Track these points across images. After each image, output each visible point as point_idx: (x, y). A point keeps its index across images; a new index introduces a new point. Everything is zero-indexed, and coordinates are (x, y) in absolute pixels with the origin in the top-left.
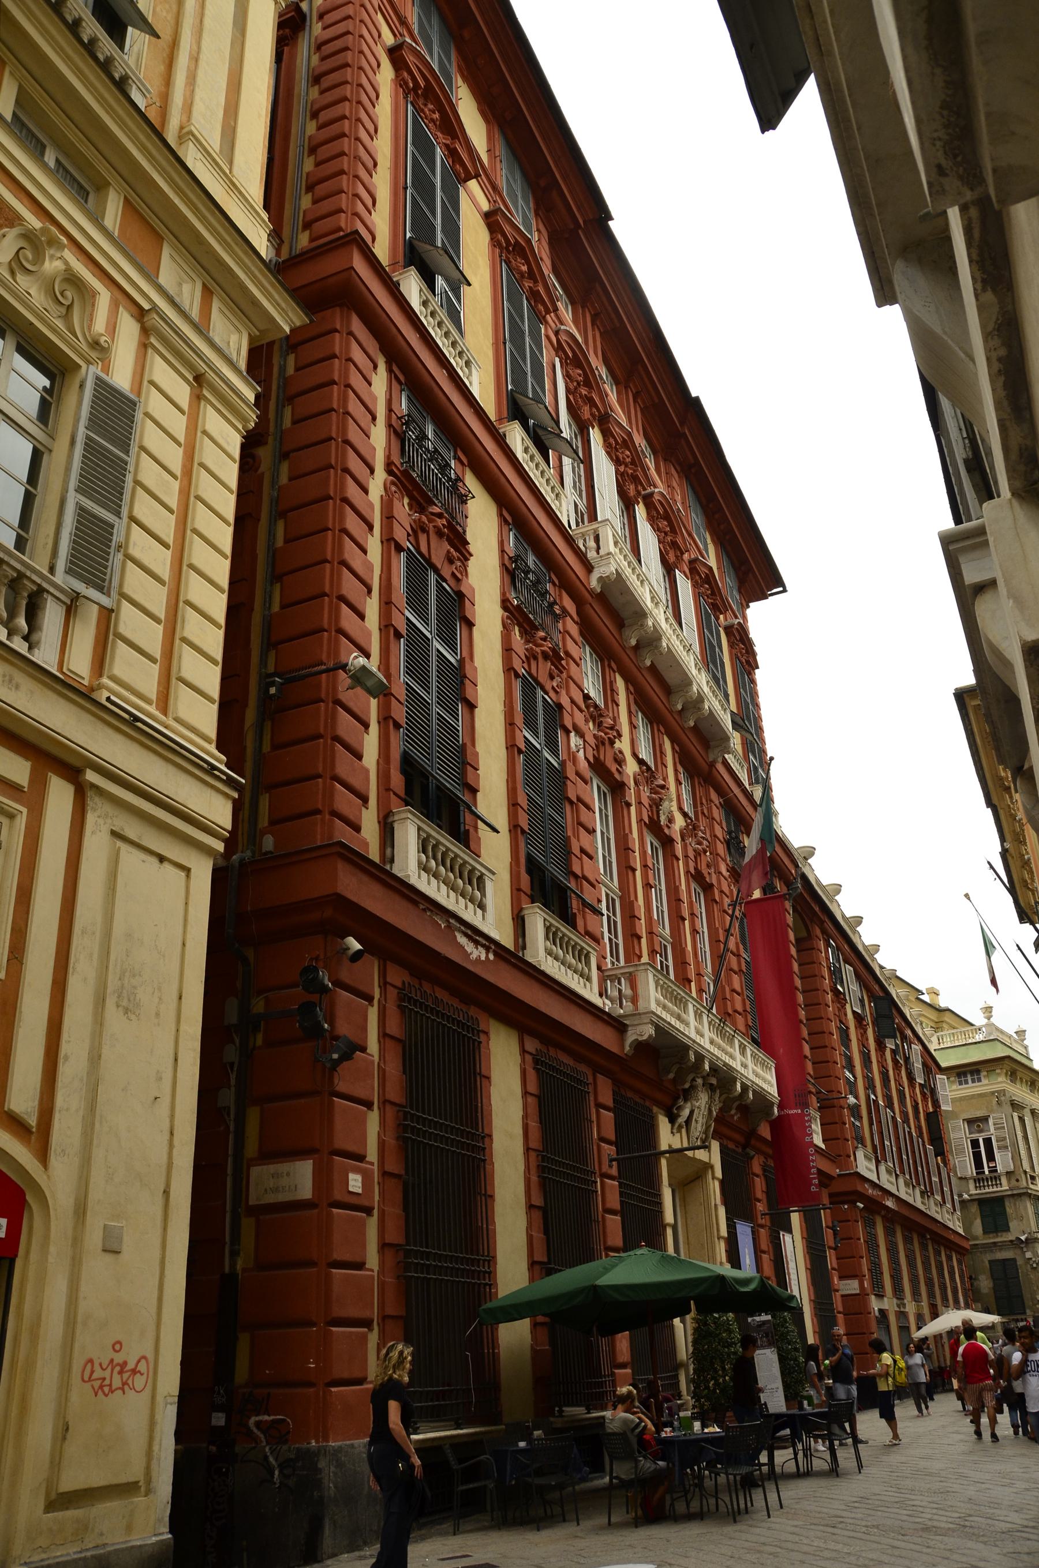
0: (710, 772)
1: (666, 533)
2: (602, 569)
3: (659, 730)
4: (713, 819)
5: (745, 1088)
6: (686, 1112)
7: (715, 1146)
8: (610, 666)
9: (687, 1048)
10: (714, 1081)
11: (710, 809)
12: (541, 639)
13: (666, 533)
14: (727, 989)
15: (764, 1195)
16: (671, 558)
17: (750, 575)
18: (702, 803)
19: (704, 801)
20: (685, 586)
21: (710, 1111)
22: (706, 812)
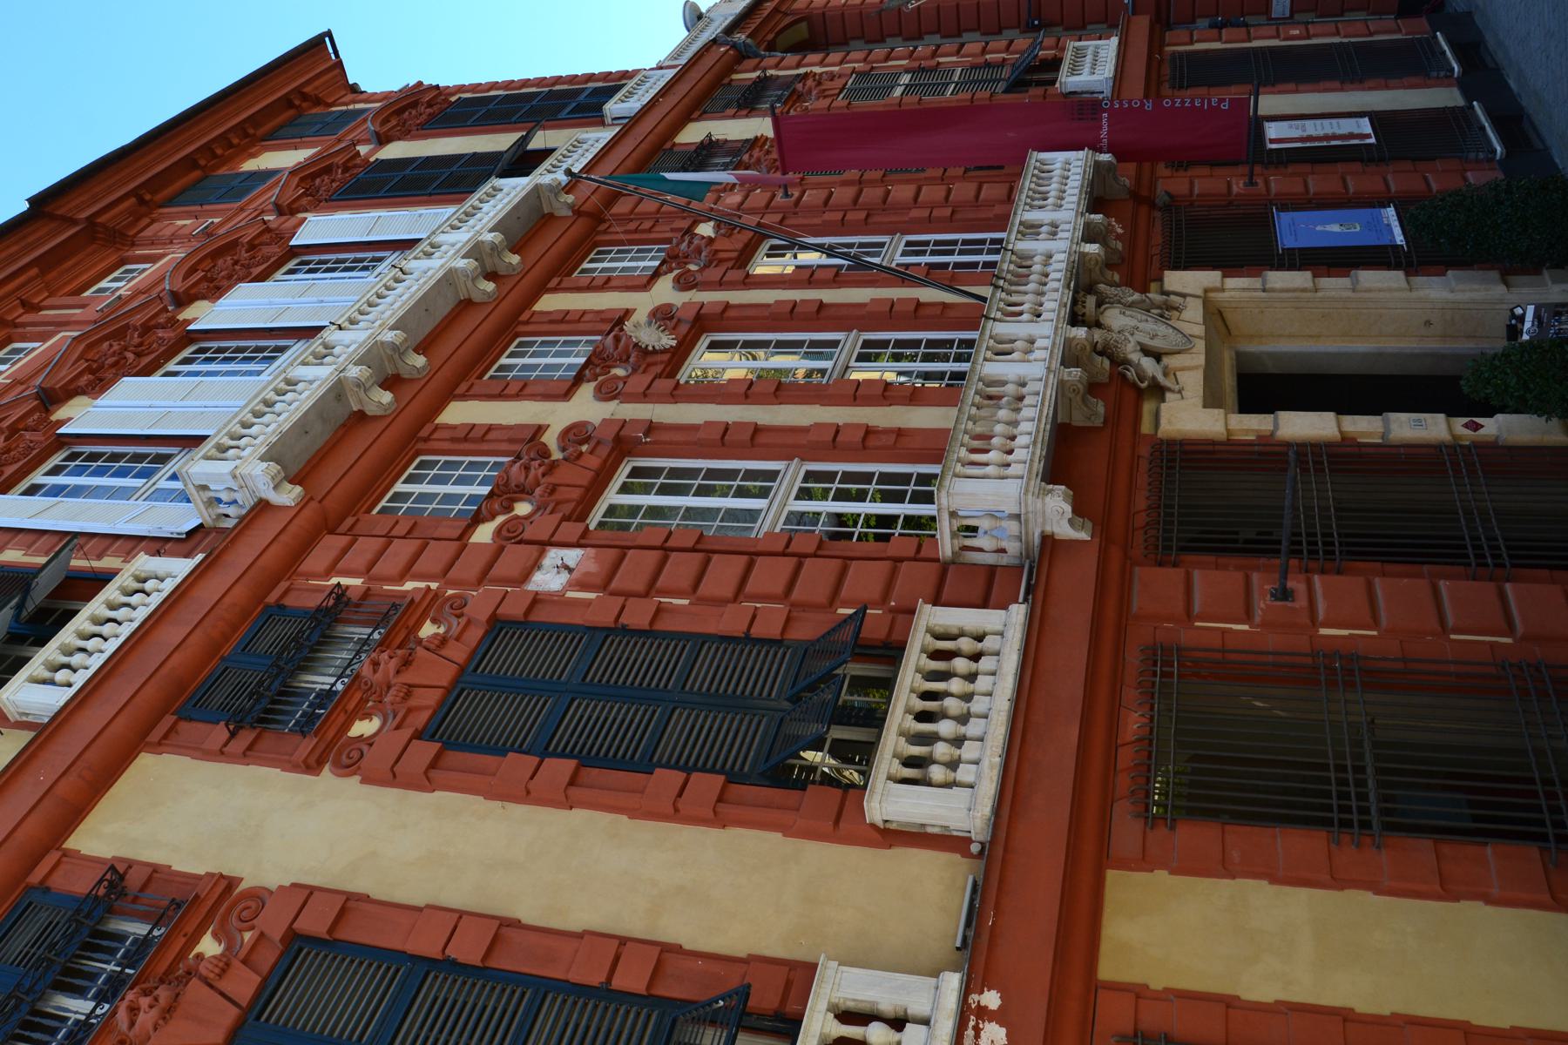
0: (588, 214)
1: (236, 263)
2: (261, 486)
3: (527, 323)
4: (658, 211)
5: (1089, 235)
6: (1148, 364)
7: (1176, 280)
8: (426, 440)
9: (1061, 384)
10: (1091, 301)
11: (644, 216)
12: (375, 671)
13: (236, 263)
14: (915, 213)
15: (1219, 171)
16: (275, 250)
17: (307, 90)
18: (636, 231)
19: (632, 226)
20: (318, 228)
21: (1131, 305)
22: (647, 225)
